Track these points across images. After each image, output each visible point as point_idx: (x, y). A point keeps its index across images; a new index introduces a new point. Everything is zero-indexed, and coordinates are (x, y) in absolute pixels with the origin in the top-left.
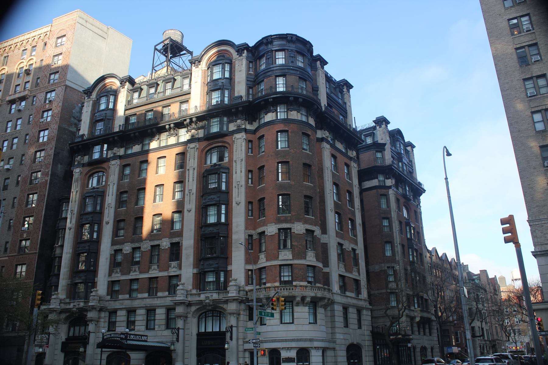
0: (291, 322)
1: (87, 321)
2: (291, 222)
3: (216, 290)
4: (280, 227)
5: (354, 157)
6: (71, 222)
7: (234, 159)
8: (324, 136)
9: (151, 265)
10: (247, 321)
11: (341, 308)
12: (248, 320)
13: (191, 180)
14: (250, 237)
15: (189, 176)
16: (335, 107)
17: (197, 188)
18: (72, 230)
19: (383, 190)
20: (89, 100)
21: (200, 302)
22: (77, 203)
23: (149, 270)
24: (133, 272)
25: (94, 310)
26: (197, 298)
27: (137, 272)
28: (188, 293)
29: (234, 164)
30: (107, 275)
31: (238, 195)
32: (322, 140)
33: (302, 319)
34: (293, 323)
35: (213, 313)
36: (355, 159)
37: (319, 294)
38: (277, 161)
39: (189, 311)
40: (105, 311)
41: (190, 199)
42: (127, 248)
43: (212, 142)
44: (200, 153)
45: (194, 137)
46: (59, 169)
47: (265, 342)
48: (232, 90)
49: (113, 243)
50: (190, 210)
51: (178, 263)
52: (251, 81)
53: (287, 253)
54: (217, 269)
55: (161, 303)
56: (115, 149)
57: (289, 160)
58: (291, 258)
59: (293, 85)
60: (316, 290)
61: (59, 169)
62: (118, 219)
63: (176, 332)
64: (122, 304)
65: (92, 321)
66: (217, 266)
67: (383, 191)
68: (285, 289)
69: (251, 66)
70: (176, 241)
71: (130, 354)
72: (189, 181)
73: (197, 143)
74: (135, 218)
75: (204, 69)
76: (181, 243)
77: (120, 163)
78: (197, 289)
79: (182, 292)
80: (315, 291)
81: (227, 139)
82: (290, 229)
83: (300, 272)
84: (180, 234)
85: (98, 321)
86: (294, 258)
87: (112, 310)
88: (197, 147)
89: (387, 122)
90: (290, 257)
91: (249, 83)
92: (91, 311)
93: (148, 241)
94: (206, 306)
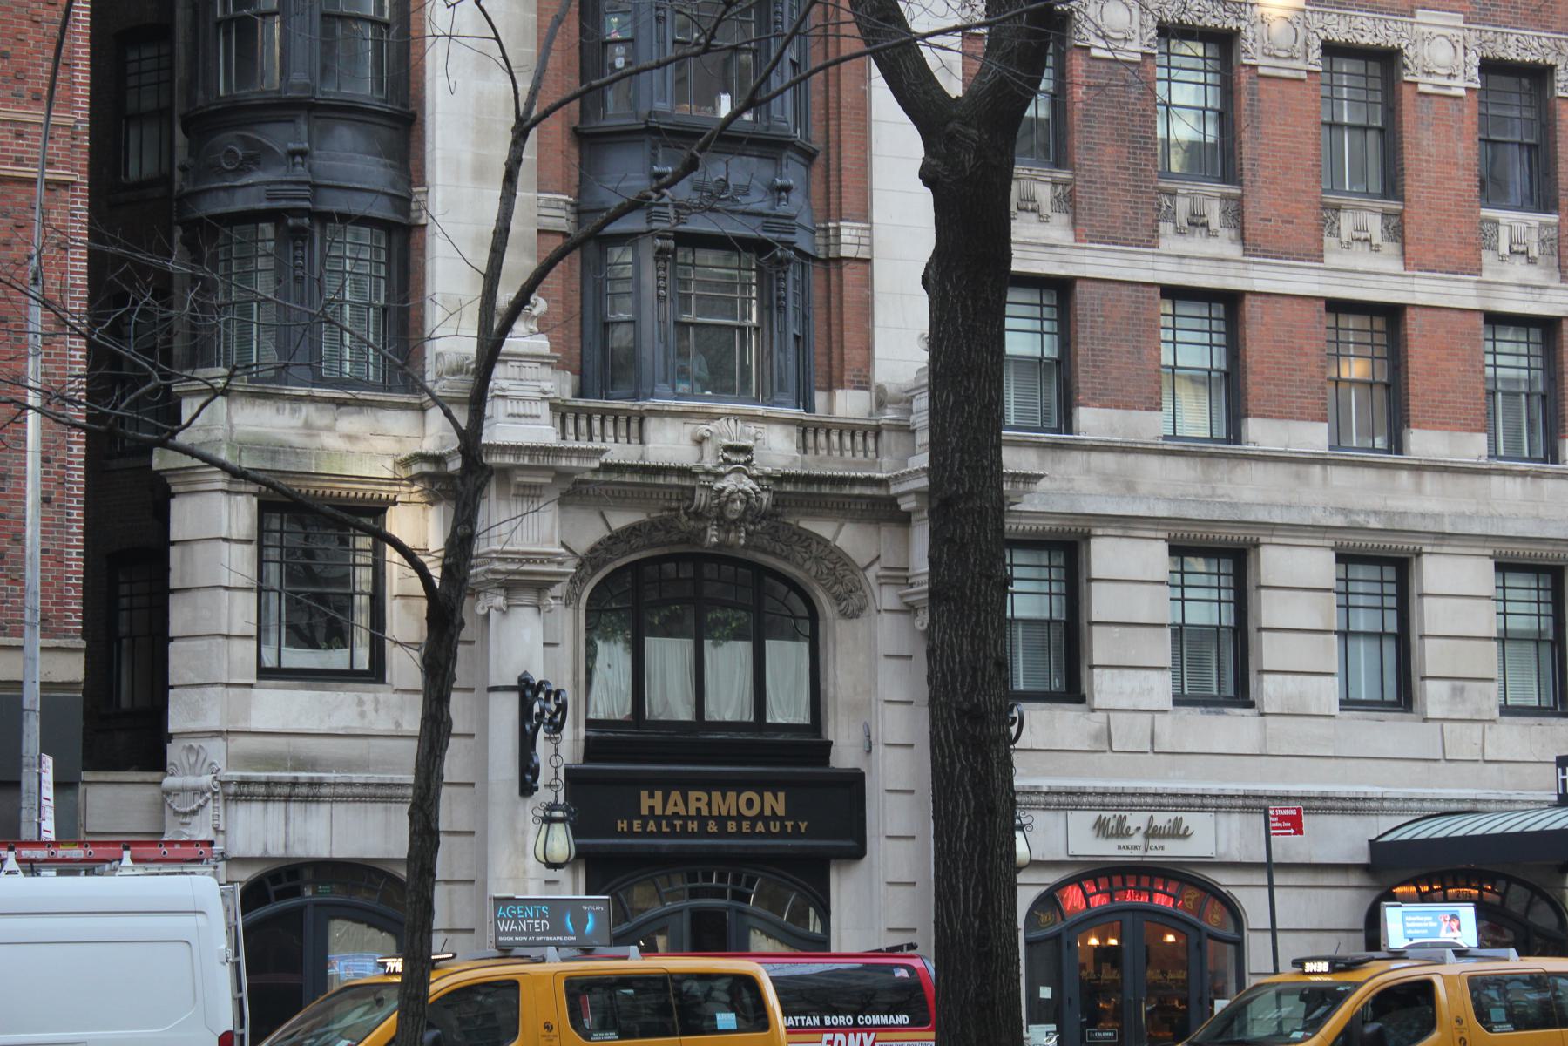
24: (1179, 232)
27: (1211, 234)
51: (1543, 225)
64: (1130, 487)
70: (1529, 58)
71: (1235, 892)
87: (1052, 524)
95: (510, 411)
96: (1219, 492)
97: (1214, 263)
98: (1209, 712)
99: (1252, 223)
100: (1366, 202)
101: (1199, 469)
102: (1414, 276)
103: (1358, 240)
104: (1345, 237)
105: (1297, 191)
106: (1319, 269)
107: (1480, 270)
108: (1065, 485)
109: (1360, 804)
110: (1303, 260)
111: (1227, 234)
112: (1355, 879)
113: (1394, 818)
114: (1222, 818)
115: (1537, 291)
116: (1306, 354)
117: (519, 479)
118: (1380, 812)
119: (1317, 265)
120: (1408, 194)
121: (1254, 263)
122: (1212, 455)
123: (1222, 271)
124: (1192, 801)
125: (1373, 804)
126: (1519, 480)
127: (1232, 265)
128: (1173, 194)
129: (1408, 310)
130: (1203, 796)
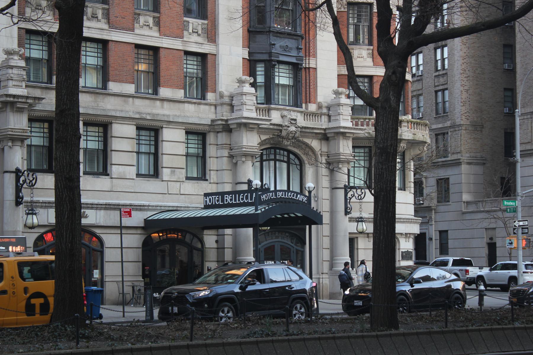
3: (292, 106)
21: (276, 127)
24: (88, 19)
25: (8, 109)
27: (99, 21)
35: (275, 155)
51: (203, 24)
71: (101, 235)
87: (45, 114)
95: (14, 84)
96: (100, 105)
97: (99, 30)
98: (94, 177)
99: (112, 18)
100: (148, 13)
101: (93, 98)
102: (163, 38)
103: (145, 25)
104: (141, 24)
105: (126, 8)
106: (133, 34)
107: (183, 37)
108: (49, 101)
109: (142, 208)
110: (128, 31)
111: (103, 20)
112: (139, 231)
113: (152, 212)
114: (98, 211)
115: (200, 45)
116: (128, 62)
117: (18, 106)
118: (148, 210)
119: (132, 33)
120: (161, 11)
121: (112, 31)
122: (97, 93)
123: (102, 33)
124: (89, 206)
125: (146, 208)
126: (193, 105)
127: (105, 31)
129: (161, 49)
130: (92, 204)
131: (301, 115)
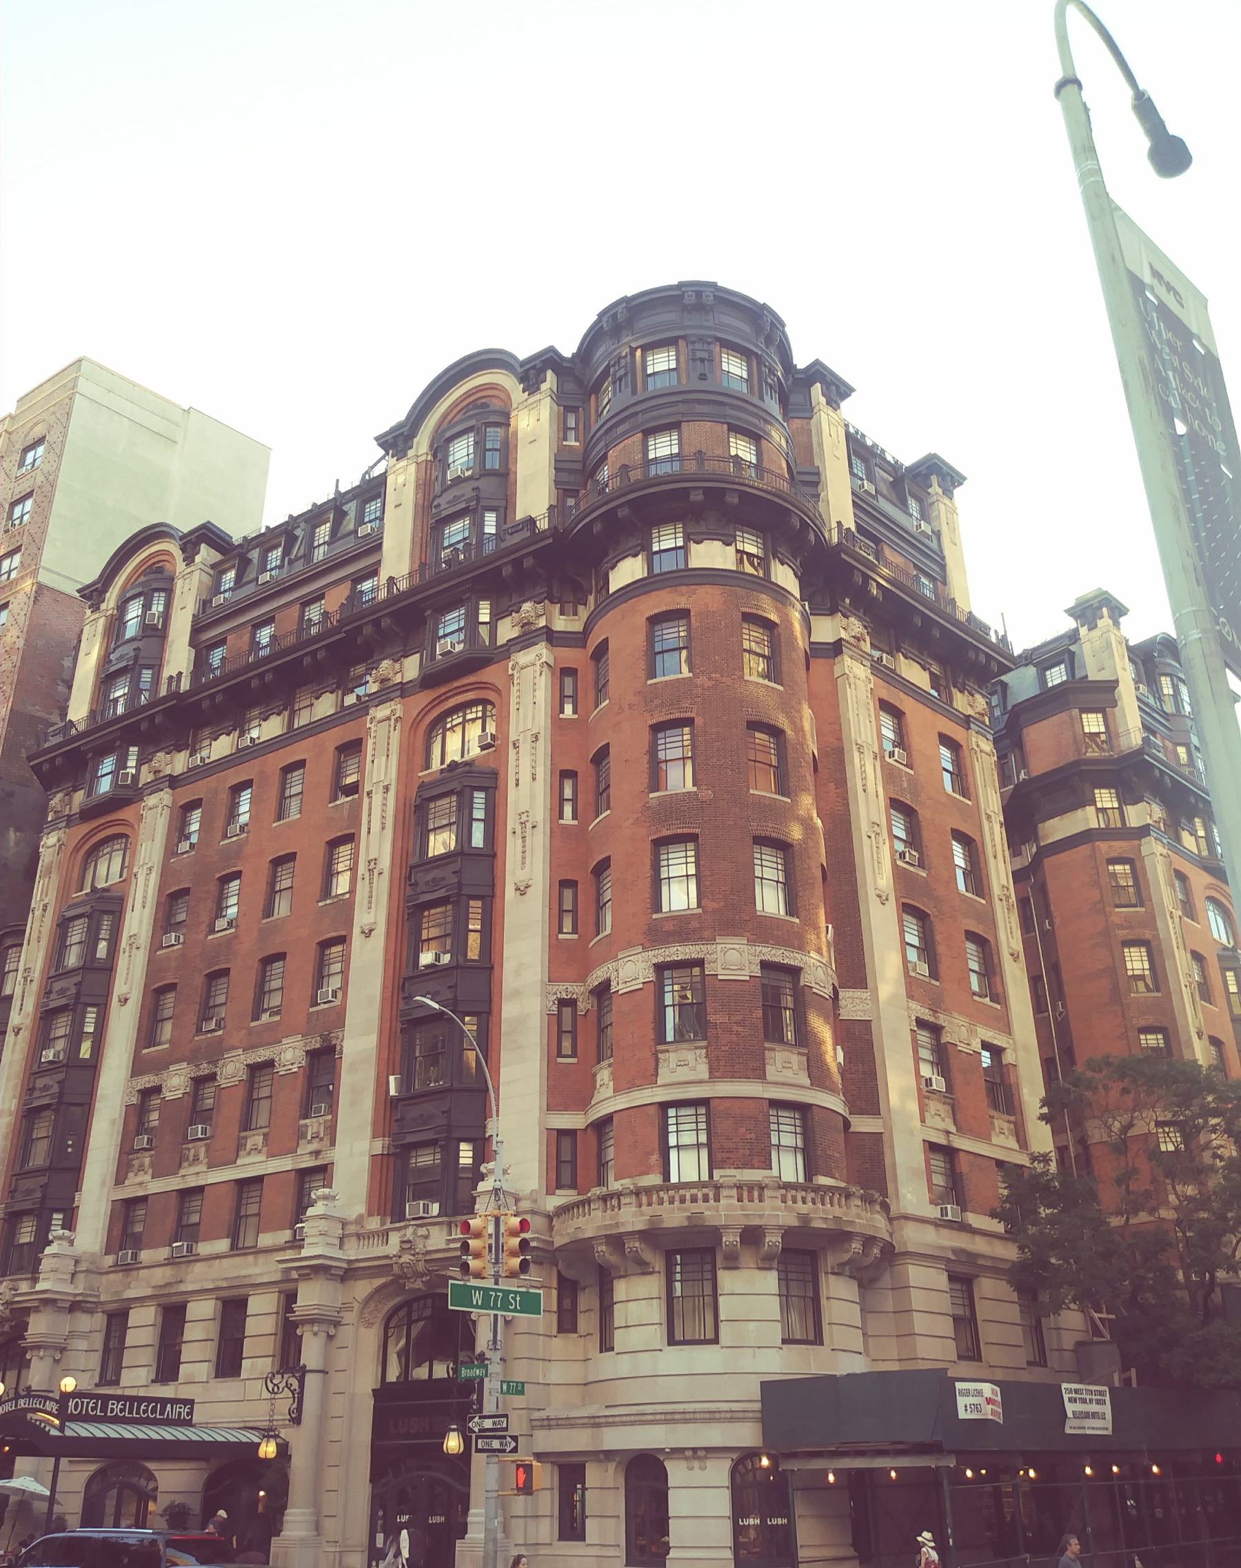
0: (710, 1335)
1: (25, 1350)
2: (702, 939)
4: (661, 959)
5: (977, 716)
6: (21, 1009)
7: (512, 737)
8: (843, 635)
9: (243, 1134)
10: (550, 1336)
11: (940, 1279)
12: (555, 1332)
13: (376, 826)
14: (567, 1011)
15: (370, 815)
16: (892, 541)
17: (393, 853)
18: (25, 1034)
19: (1113, 843)
20: (97, 615)
22: (44, 942)
23: (237, 1156)
24: (190, 1165)
26: (376, 1249)
28: (348, 1232)
29: (512, 752)
30: (110, 1180)
31: (524, 858)
32: (836, 648)
33: (751, 1324)
34: (715, 1341)
36: (983, 723)
37: (823, 1215)
38: (650, 723)
39: (351, 1300)
40: (91, 1312)
41: (371, 892)
42: (176, 1082)
43: (443, 690)
44: (407, 734)
45: (391, 683)
46: (12, 843)
47: (608, 1425)
48: (505, 506)
49: (139, 1067)
50: (371, 931)
52: (570, 471)
53: (690, 1056)
54: (445, 1135)
55: (262, 1274)
56: (161, 755)
57: (693, 715)
58: (706, 1076)
59: (700, 452)
60: (804, 1202)
61: (12, 843)
62: (156, 986)
63: (288, 1386)
65: (38, 1347)
66: (445, 1122)
67: (1119, 847)
68: (677, 1198)
69: (571, 422)
72: (369, 832)
73: (398, 700)
74: (206, 975)
75: (423, 458)
76: (338, 1048)
77: (174, 801)
78: (385, 1214)
79: (323, 1225)
80: (800, 1203)
81: (489, 674)
82: (700, 963)
83: (742, 1130)
84: (338, 1020)
85: (63, 1350)
86: (715, 1073)
88: (397, 715)
89: (1118, 611)
90: (703, 1071)
91: (565, 477)
92: (39, 1311)
93: (240, 1051)
94: (404, 1276)
100: (255, 1132)
128: (189, 1149)
131: (441, 1230)
